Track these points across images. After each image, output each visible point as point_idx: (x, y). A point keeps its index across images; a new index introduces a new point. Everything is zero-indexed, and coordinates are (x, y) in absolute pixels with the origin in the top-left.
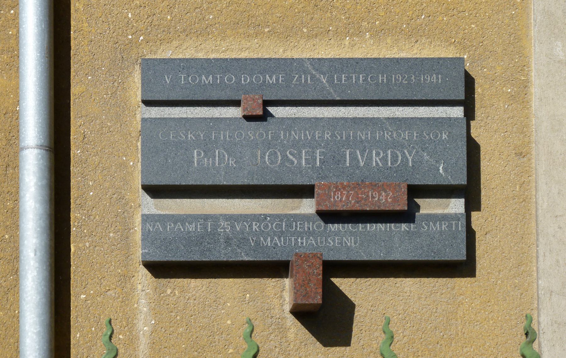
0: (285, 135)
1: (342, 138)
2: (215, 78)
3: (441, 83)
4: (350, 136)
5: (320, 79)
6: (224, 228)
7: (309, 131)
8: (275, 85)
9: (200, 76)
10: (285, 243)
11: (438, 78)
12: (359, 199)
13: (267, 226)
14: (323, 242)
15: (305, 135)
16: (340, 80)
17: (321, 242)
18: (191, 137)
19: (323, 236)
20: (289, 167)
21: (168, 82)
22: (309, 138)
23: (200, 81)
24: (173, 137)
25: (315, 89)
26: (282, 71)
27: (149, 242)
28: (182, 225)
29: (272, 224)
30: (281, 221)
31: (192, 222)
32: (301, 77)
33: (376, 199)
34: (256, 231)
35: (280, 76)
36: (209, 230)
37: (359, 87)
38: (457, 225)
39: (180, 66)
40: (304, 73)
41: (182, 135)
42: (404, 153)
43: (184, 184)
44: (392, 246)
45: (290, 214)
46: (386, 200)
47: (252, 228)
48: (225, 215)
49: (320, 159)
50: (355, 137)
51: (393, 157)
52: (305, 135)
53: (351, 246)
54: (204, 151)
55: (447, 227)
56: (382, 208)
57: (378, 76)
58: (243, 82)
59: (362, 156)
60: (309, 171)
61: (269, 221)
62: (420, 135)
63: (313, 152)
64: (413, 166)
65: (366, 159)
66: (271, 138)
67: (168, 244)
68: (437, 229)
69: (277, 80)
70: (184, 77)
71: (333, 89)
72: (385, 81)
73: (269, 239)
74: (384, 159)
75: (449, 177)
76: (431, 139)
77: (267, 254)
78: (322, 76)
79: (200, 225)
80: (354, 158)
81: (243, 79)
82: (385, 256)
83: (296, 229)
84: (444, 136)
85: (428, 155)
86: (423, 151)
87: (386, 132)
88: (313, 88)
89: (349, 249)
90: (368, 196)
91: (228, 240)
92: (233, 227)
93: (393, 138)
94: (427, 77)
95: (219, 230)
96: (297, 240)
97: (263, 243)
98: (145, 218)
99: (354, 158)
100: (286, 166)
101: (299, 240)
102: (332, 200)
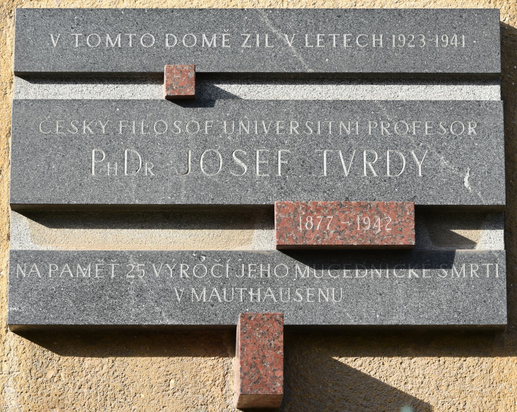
0: (229, 126)
1: (315, 132)
2: (125, 39)
3: (466, 47)
4: (328, 129)
5: (282, 41)
6: (136, 274)
7: (266, 121)
8: (216, 49)
9: (103, 35)
10: (228, 298)
11: (460, 40)
12: (342, 228)
13: (202, 270)
14: (287, 296)
15: (260, 127)
16: (313, 42)
17: (285, 296)
18: (86, 130)
19: (288, 286)
20: (235, 178)
21: (55, 45)
22: (266, 132)
23: (103, 43)
24: (59, 129)
25: (275, 56)
26: (226, 28)
27: (19, 294)
28: (71, 268)
29: (209, 268)
30: (223, 261)
31: (86, 264)
32: (254, 37)
33: (368, 228)
34: (184, 278)
35: (224, 35)
36: (113, 276)
37: (341, 50)
38: (492, 269)
39: (73, 20)
40: (260, 32)
41: (73, 126)
42: (410, 156)
43: (75, 202)
44: (394, 303)
45: (237, 252)
46: (383, 229)
47: (179, 274)
48: (138, 252)
49: (282, 164)
50: (335, 131)
51: (394, 161)
52: (260, 127)
53: (330, 302)
54: (106, 152)
55: (477, 272)
56: (377, 242)
57: (370, 37)
58: (167, 45)
59: (347, 160)
60: (266, 183)
61: (204, 263)
62: (434, 127)
63: (272, 154)
64: (424, 176)
65: (353, 166)
66: (209, 131)
67: (49, 298)
68: (462, 275)
69: (219, 41)
70: (79, 36)
71: (303, 56)
72: (381, 43)
73: (204, 291)
74: (381, 166)
75: (479, 194)
76: (450, 134)
77: (201, 314)
78: (286, 36)
79: (99, 268)
80: (334, 163)
81: (167, 40)
82: (383, 318)
83: (246, 275)
84: (471, 130)
85: (446, 159)
86: (439, 152)
87: (382, 123)
88: (273, 55)
89: (327, 306)
90: (354, 223)
91: (141, 292)
92: (149, 270)
93: (392, 132)
94: (445, 38)
95: (128, 276)
96: (247, 292)
97: (194, 297)
98: (15, 256)
99: (334, 163)
100: (231, 175)
101: (251, 293)
102: (301, 229)
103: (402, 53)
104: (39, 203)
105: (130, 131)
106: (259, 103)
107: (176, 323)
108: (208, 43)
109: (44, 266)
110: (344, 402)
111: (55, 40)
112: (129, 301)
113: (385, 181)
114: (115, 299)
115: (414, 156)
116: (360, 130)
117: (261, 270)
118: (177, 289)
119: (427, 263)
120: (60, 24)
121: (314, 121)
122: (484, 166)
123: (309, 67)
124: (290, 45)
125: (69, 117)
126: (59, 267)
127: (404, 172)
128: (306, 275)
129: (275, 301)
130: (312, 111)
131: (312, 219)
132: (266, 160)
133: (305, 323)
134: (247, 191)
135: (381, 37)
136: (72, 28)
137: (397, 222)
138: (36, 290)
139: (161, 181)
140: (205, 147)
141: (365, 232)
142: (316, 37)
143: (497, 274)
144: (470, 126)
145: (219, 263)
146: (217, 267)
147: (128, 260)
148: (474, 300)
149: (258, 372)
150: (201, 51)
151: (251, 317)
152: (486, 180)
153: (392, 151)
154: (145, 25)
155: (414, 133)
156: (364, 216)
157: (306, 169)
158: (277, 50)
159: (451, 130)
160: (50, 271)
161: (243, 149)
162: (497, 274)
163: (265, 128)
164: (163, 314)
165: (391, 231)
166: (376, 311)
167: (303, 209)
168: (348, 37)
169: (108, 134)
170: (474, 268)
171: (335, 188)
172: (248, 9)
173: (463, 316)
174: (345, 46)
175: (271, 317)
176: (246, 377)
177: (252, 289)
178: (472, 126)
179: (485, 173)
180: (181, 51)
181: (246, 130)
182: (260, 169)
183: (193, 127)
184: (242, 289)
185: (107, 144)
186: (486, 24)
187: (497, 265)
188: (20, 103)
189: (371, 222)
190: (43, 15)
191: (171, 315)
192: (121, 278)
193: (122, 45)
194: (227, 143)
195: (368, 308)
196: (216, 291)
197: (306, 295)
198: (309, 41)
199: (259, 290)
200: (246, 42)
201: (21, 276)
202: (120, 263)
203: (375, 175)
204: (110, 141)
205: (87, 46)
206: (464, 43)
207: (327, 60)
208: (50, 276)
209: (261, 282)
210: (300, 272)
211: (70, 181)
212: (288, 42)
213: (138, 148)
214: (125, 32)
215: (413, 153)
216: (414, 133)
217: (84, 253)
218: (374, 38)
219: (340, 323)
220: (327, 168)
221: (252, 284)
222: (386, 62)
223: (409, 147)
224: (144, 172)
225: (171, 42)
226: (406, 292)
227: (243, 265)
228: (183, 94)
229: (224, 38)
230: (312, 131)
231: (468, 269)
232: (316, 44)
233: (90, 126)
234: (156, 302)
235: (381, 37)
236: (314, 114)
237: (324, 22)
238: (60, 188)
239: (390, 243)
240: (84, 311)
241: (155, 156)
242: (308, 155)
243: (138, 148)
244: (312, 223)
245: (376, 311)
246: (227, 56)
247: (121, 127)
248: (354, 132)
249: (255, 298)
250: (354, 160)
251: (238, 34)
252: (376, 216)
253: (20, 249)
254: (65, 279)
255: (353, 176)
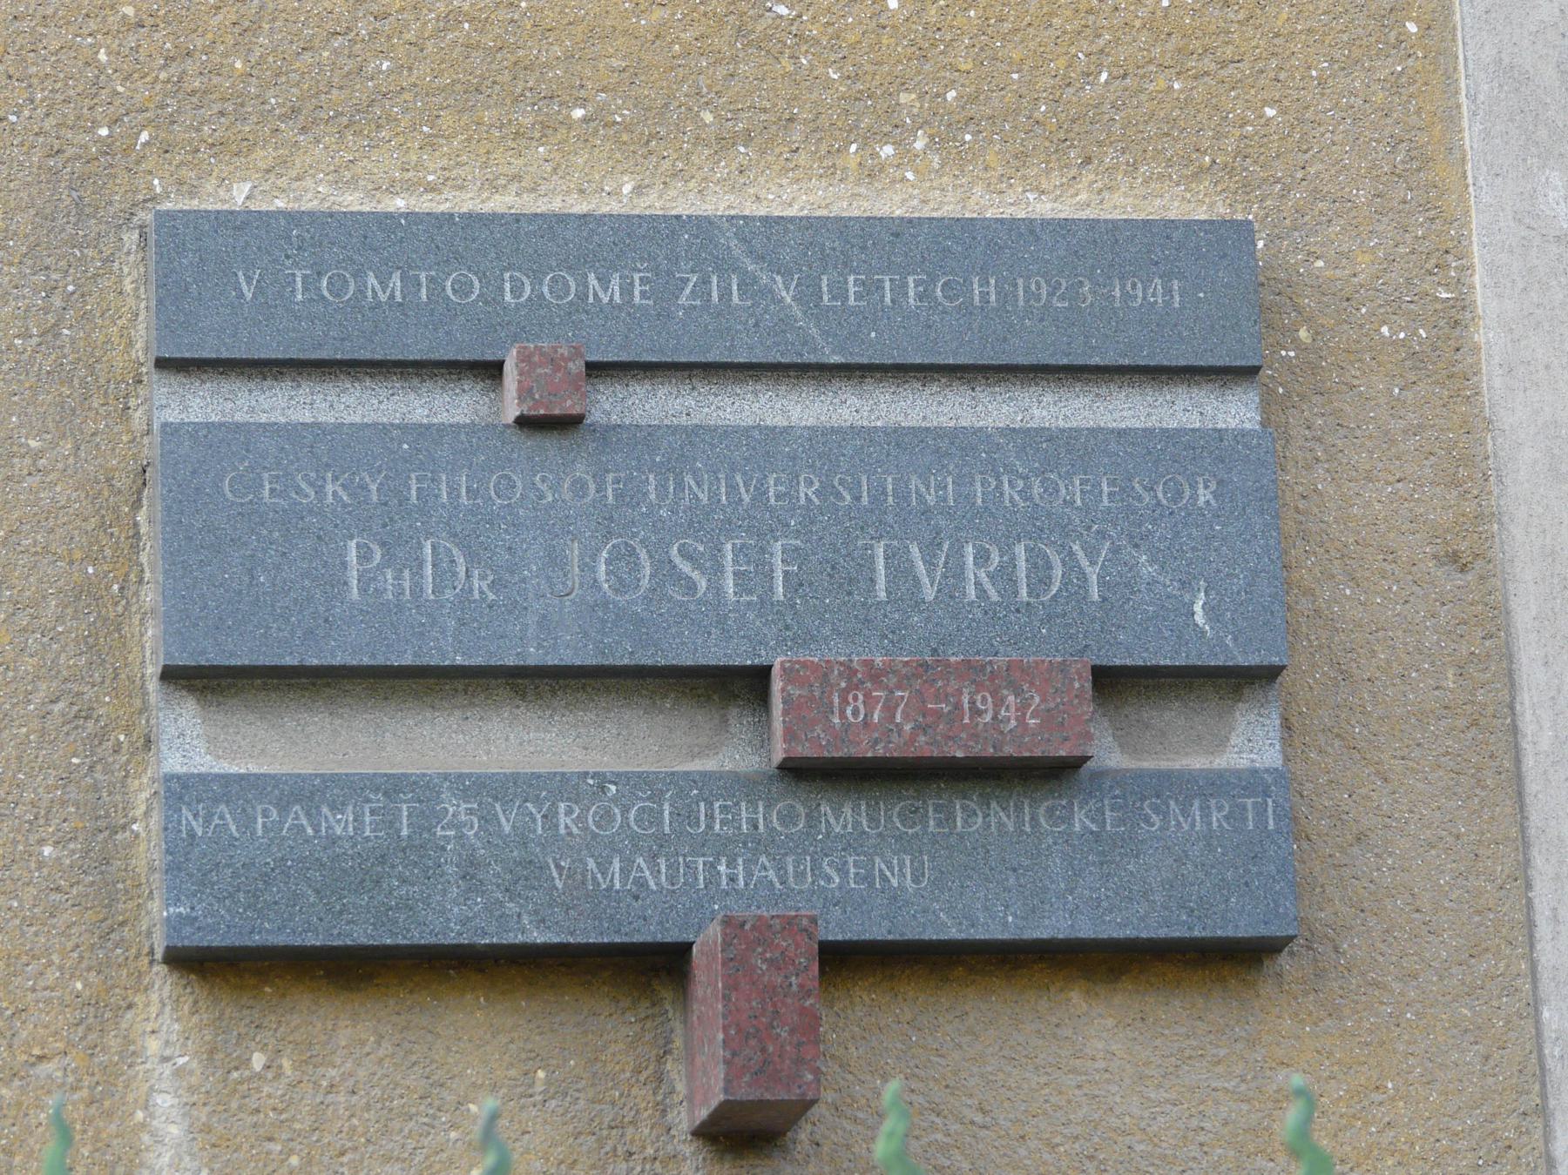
0: (662, 487)
1: (858, 498)
2: (411, 283)
3: (1183, 307)
4: (884, 493)
5: (771, 291)
6: (458, 826)
7: (744, 474)
8: (620, 307)
9: (359, 274)
10: (672, 880)
11: (1168, 291)
12: (929, 719)
13: (607, 816)
14: (804, 873)
15: (732, 488)
16: (840, 293)
17: (800, 876)
18: (335, 493)
19: (805, 852)
20: (681, 604)
21: (249, 296)
22: (746, 498)
23: (361, 291)
24: (272, 490)
25: (756, 325)
26: (642, 259)
27: (191, 875)
28: (308, 815)
29: (625, 810)
30: (657, 797)
31: (343, 804)
32: (706, 281)
33: (988, 718)
34: (570, 834)
35: (637, 276)
36: (405, 832)
37: (906, 314)
38: (1261, 812)
39: (290, 238)
40: (718, 269)
41: (303, 485)
42: (1071, 553)
43: (315, 662)
44: (1045, 890)
45: (687, 773)
46: (1021, 720)
47: (557, 826)
48: (460, 776)
49: (786, 573)
50: (902, 496)
51: (1035, 566)
52: (732, 488)
53: (901, 887)
54: (383, 544)
55: (1227, 818)
56: (1009, 750)
57: (967, 282)
58: (508, 297)
59: (930, 565)
60: (751, 615)
61: (614, 800)
62: (1123, 490)
63: (763, 550)
64: (1104, 599)
65: (944, 576)
66: (616, 497)
67: (261, 885)
68: (1193, 825)
69: (627, 290)
70: (305, 277)
71: (817, 326)
72: (993, 298)
73: (616, 865)
74: (1005, 575)
75: (1229, 640)
76: (1159, 504)
77: (612, 918)
78: (779, 278)
79: (372, 812)
80: (900, 570)
81: (507, 286)
82: (1021, 923)
83: (710, 827)
84: (1204, 496)
85: (1152, 562)
86: (1136, 546)
87: (1005, 479)
88: (751, 322)
89: (895, 897)
90: (958, 706)
91: (470, 870)
92: (487, 819)
93: (1029, 499)
94: (1134, 286)
95: (439, 833)
96: (713, 866)
97: (594, 878)
98: (175, 786)
99: (900, 570)
100: (670, 599)
101: (722, 868)
102: (836, 721)
103: (1042, 320)
104: (233, 663)
105: (437, 496)
106: (727, 432)
107: (556, 940)
108: (601, 294)
109: (244, 810)
110: (933, 1117)
111: (249, 283)
112: (444, 890)
113: (1018, 611)
114: (413, 885)
115: (1081, 554)
116: (957, 495)
117: (744, 814)
118: (555, 860)
119: (1116, 797)
120: (259, 248)
121: (852, 475)
122: (1237, 576)
123: (833, 352)
124: (789, 300)
125: (292, 462)
126: (279, 815)
127: (1060, 590)
128: (845, 827)
129: (778, 885)
130: (849, 451)
131: (861, 697)
132: (748, 563)
133: (848, 936)
134: (709, 633)
135: (992, 281)
136: (288, 257)
137: (1052, 705)
138: (228, 866)
139: (510, 612)
140: (609, 535)
141: (980, 727)
142: (846, 282)
143: (1271, 822)
144: (1201, 486)
145: (649, 799)
146: (643, 808)
147: (439, 793)
148: (1223, 880)
149: (763, 1050)
150: (587, 312)
151: (743, 924)
152: (1241, 610)
153: (1032, 544)
154: (457, 252)
155: (1079, 503)
156: (978, 692)
157: (841, 585)
158: (759, 311)
159: (1160, 495)
160: (260, 820)
161: (696, 539)
162: (1271, 822)
163: (743, 490)
164: (525, 920)
165: (1040, 726)
166: (1007, 907)
167: (840, 674)
168: (917, 283)
169: (386, 504)
170: (1220, 809)
171: (906, 628)
172: (689, 217)
173: (1199, 918)
174: (911, 301)
175: (789, 923)
176: (736, 1060)
177: (724, 860)
178: (1206, 487)
179: (1239, 593)
180: (542, 313)
181: (701, 496)
182: (736, 585)
183: (579, 487)
184: (701, 860)
185: (385, 526)
186: (1225, 255)
187: (1270, 801)
188: (177, 430)
189: (995, 705)
190: (219, 225)
191: (543, 921)
192: (425, 835)
193: (404, 298)
194: (659, 525)
195: (987, 899)
196: (643, 865)
197: (848, 872)
198: (830, 291)
199: (740, 861)
200: (688, 291)
201: (192, 835)
202: (420, 802)
203: (995, 597)
204: (391, 519)
205: (323, 297)
206: (1177, 298)
207: (873, 334)
208: (260, 833)
209: (745, 844)
210: (832, 820)
211: (300, 612)
212: (784, 294)
213: (456, 535)
214: (410, 268)
215: (1076, 547)
216: (1079, 503)
217: (334, 779)
218: (976, 286)
219: (926, 937)
220: (888, 582)
221: (724, 848)
222: (1005, 339)
223: (1067, 535)
224: (471, 590)
225: (517, 291)
226: (1071, 864)
227: (702, 804)
228: (557, 412)
229: (637, 282)
230: (848, 498)
231: (1206, 815)
232: (847, 298)
233: (342, 485)
234: (507, 890)
235: (992, 281)
236: (852, 457)
237: (863, 248)
238: (279, 629)
239: (1038, 753)
240: (341, 913)
241: (495, 554)
242: (844, 552)
243: (456, 535)
244: (861, 707)
245: (1007, 907)
246: (646, 325)
247: (414, 488)
248: (945, 500)
249: (732, 880)
250: (946, 563)
251: (669, 273)
252: (1005, 692)
253: (184, 769)
254: (295, 840)
255: (947, 599)
